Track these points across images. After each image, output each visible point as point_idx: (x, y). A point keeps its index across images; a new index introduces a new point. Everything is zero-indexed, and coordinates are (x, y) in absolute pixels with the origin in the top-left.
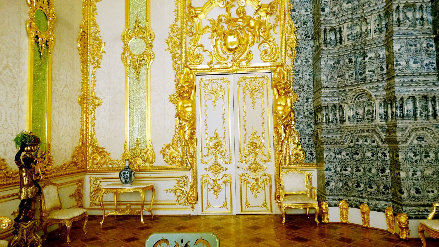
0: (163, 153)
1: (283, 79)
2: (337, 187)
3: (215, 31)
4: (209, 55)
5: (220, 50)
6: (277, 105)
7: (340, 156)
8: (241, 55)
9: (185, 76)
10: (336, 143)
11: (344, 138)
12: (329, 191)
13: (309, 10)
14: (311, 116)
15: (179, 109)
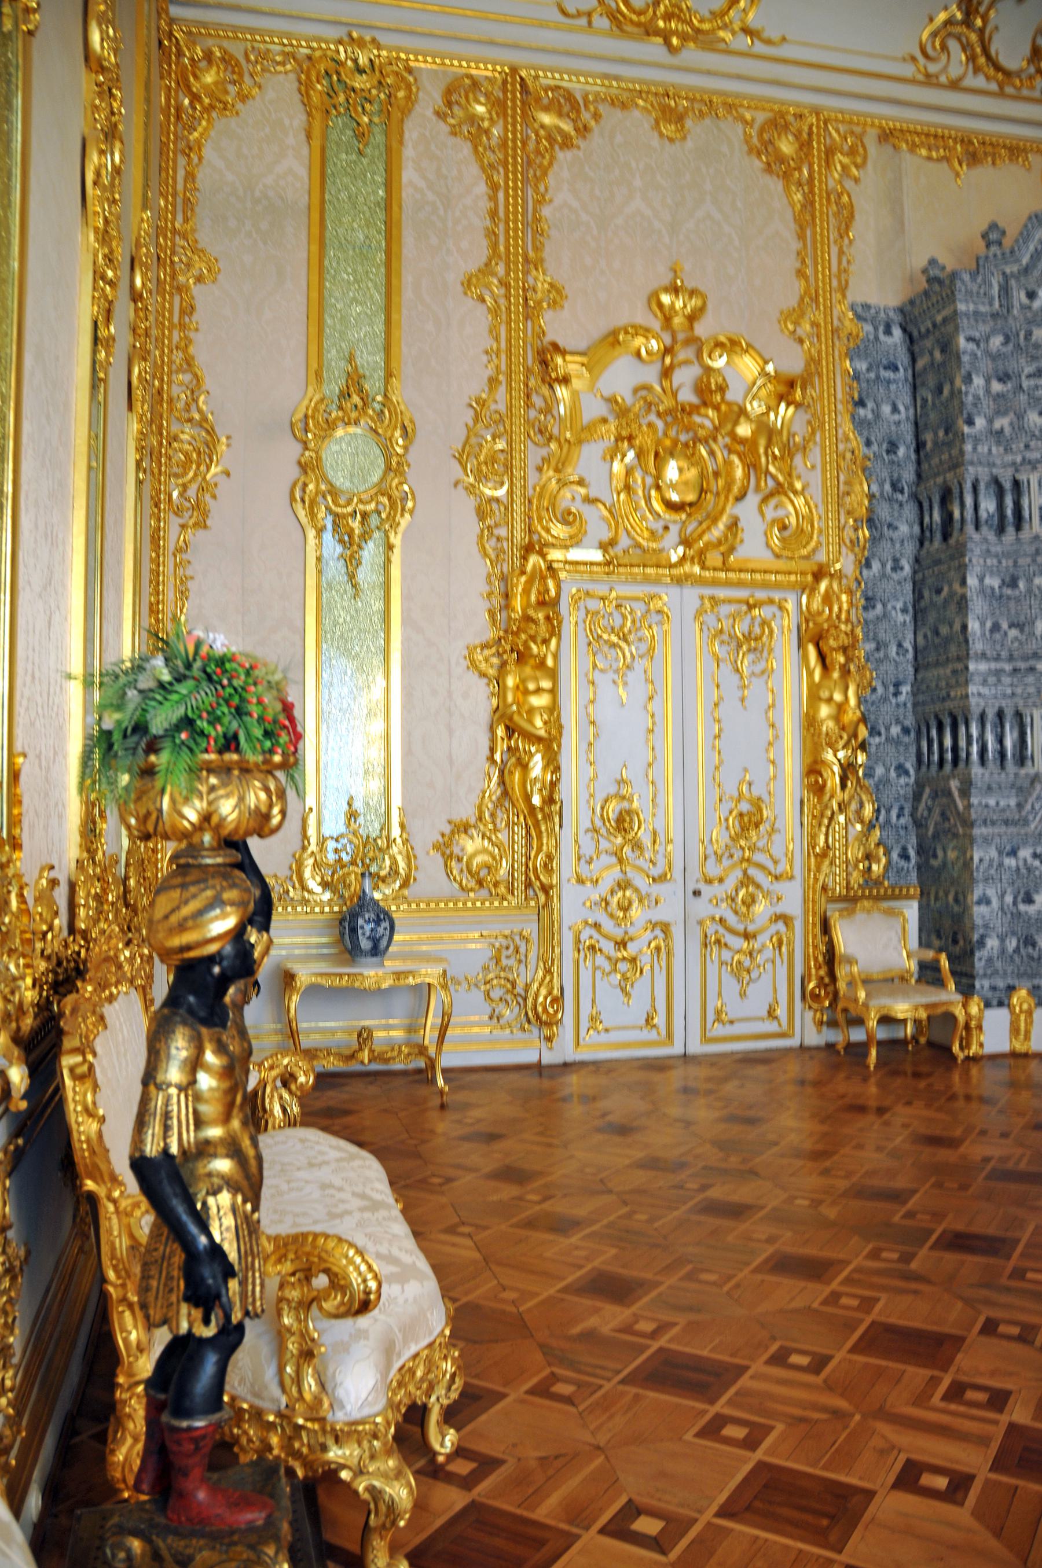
0: (446, 849)
1: (838, 617)
2: (1003, 951)
3: (630, 438)
4: (603, 518)
5: (643, 503)
6: (814, 698)
7: (1010, 862)
8: (709, 528)
9: (530, 583)
10: (1006, 822)
11: (1028, 807)
12: (983, 962)
13: (902, 408)
14: (906, 739)
15: (510, 698)
